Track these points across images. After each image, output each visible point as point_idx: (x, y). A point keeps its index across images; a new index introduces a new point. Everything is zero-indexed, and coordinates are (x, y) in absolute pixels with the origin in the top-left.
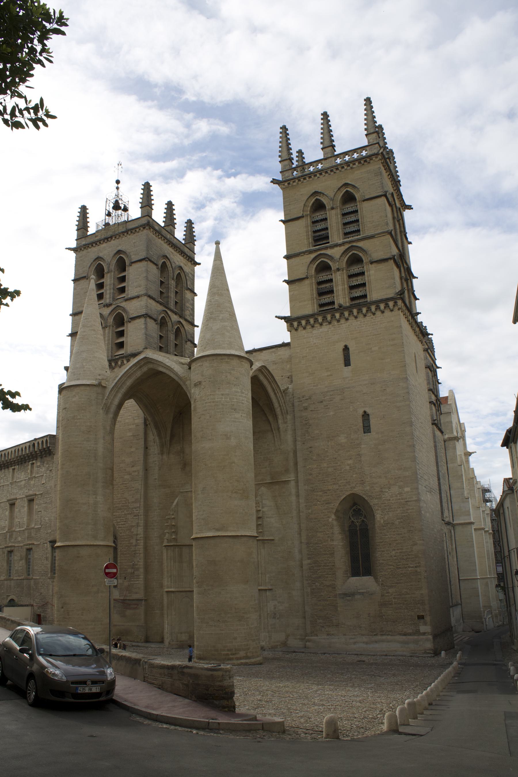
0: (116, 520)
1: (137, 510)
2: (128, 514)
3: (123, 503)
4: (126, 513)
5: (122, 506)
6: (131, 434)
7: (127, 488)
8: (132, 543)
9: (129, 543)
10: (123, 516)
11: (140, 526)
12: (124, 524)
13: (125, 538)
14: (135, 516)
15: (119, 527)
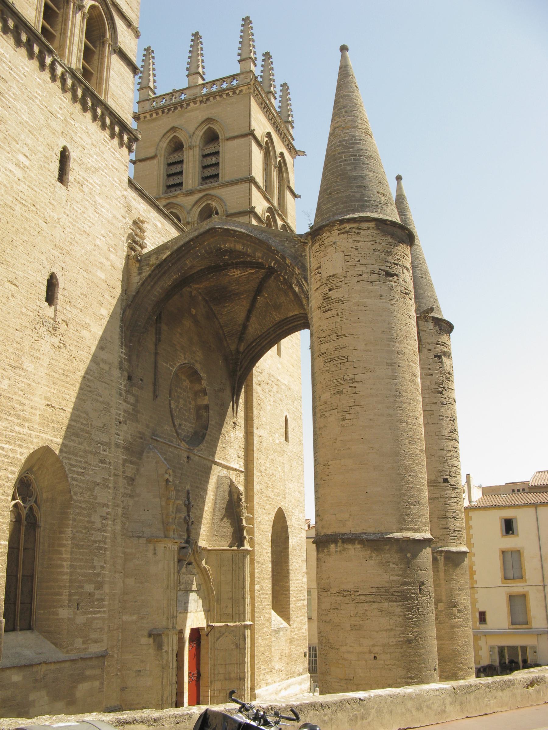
0: (69, 459)
1: (105, 451)
2: (91, 452)
3: (82, 424)
4: (87, 448)
5: (80, 429)
6: (103, 278)
7: (91, 392)
8: (94, 523)
9: (89, 522)
10: (81, 453)
11: (108, 487)
12: (82, 474)
13: (84, 509)
14: (101, 461)
15: (73, 479)
